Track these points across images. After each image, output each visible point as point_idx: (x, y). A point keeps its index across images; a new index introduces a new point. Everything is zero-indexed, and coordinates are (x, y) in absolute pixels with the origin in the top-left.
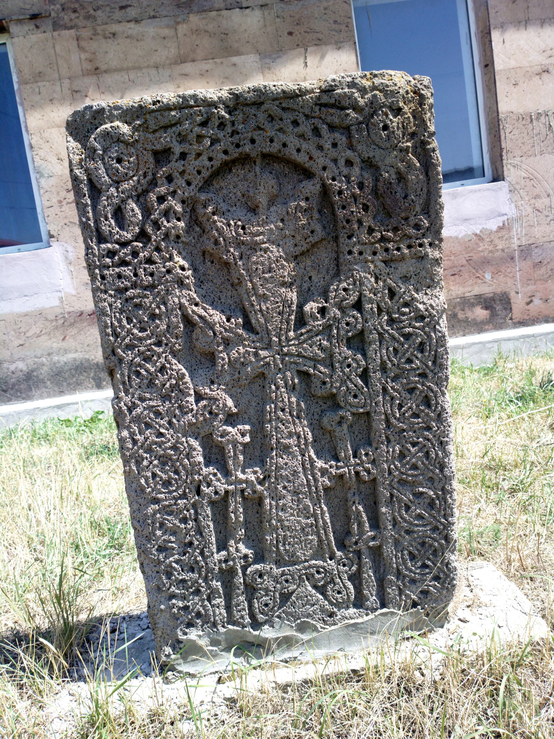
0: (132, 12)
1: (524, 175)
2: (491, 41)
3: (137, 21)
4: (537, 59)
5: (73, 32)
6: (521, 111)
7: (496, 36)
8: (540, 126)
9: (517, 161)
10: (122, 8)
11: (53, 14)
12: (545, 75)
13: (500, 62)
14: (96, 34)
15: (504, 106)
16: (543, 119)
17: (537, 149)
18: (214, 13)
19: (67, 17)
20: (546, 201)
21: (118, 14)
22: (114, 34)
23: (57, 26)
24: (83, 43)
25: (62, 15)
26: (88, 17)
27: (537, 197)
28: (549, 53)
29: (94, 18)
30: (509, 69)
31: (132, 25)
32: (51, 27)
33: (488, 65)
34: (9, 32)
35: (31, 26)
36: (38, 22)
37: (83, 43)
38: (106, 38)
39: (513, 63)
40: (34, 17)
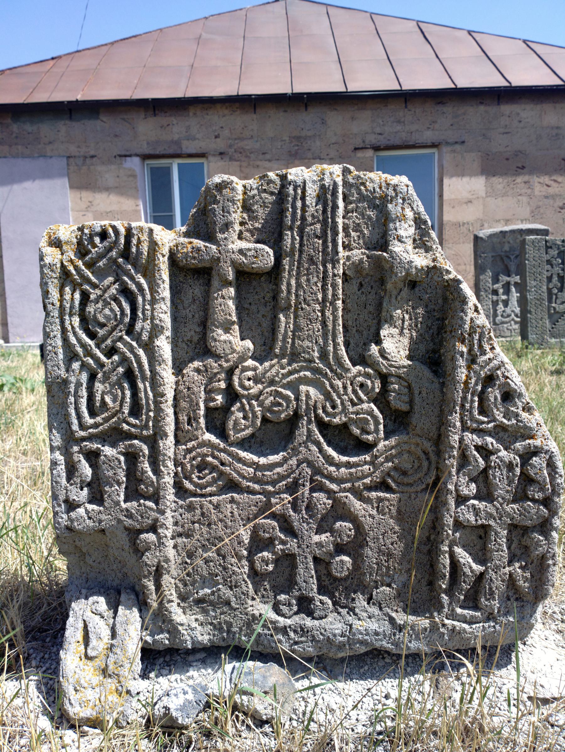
0: (268, 156)
1: (453, 253)
2: (442, 185)
3: (270, 161)
4: (466, 195)
5: (238, 163)
6: (455, 221)
7: (446, 181)
8: (464, 229)
9: (450, 245)
10: (264, 154)
11: (230, 153)
12: (469, 204)
13: (445, 197)
14: (249, 165)
15: (446, 218)
16: (466, 226)
17: (461, 240)
18: (306, 161)
19: (237, 155)
20: (464, 267)
21: (261, 157)
22: (258, 166)
23: (231, 159)
24: (243, 169)
25: (234, 154)
26: (247, 156)
27: (459, 265)
28: (472, 193)
29: (249, 157)
30: (451, 200)
31: (267, 162)
32: (228, 159)
33: (441, 196)
34: (207, 158)
35: (219, 158)
36: (223, 156)
37: (243, 169)
38: (254, 167)
39: (453, 197)
40: (221, 154)
